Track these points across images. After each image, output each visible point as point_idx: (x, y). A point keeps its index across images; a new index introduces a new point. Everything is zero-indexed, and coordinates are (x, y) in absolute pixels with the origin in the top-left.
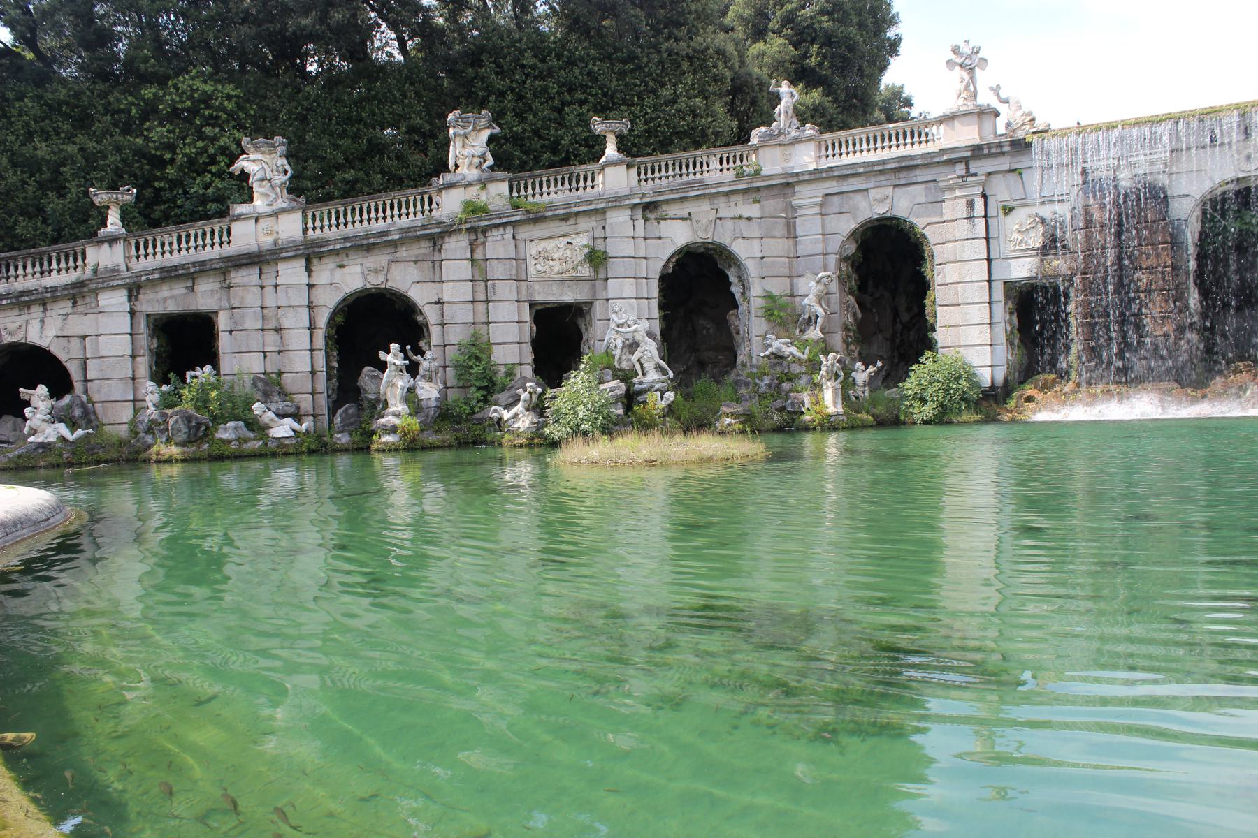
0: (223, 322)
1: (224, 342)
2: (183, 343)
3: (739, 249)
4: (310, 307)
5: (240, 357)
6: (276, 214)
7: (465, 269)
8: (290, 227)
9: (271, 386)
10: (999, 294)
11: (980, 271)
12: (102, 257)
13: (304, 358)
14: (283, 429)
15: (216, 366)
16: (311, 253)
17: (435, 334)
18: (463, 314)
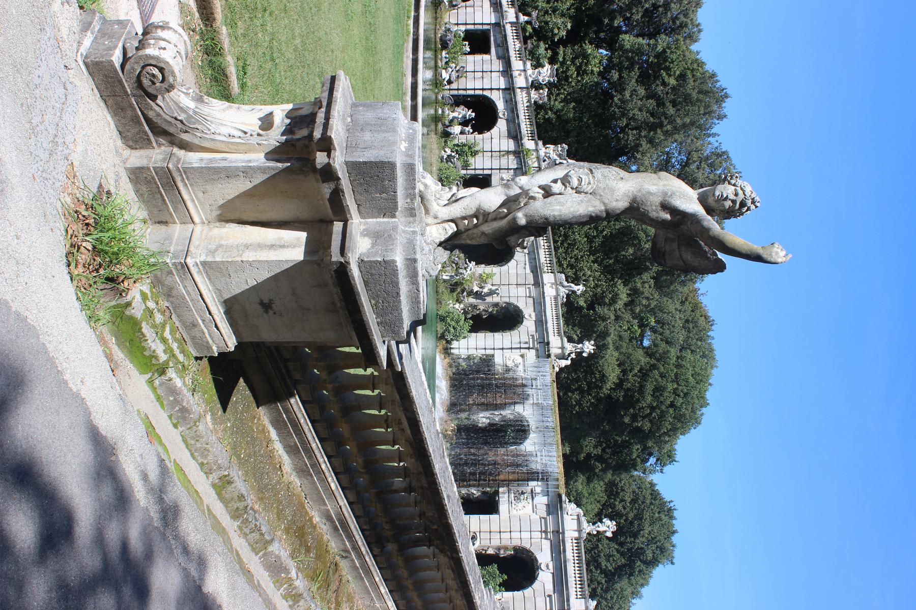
0: (486, 57)
1: (478, 57)
2: (478, 41)
3: (512, 263)
4: (491, 89)
5: (473, 62)
6: (527, 79)
7: (504, 148)
8: (520, 82)
9: (461, 73)
10: (489, 352)
11: (498, 345)
12: (511, 14)
13: (472, 85)
14: (445, 75)
15: (469, 53)
16: (510, 90)
17: (481, 136)
18: (487, 147)
